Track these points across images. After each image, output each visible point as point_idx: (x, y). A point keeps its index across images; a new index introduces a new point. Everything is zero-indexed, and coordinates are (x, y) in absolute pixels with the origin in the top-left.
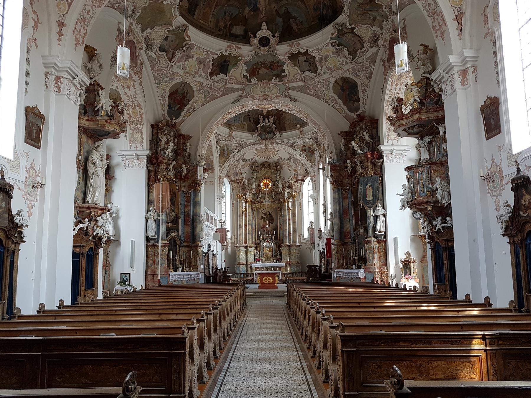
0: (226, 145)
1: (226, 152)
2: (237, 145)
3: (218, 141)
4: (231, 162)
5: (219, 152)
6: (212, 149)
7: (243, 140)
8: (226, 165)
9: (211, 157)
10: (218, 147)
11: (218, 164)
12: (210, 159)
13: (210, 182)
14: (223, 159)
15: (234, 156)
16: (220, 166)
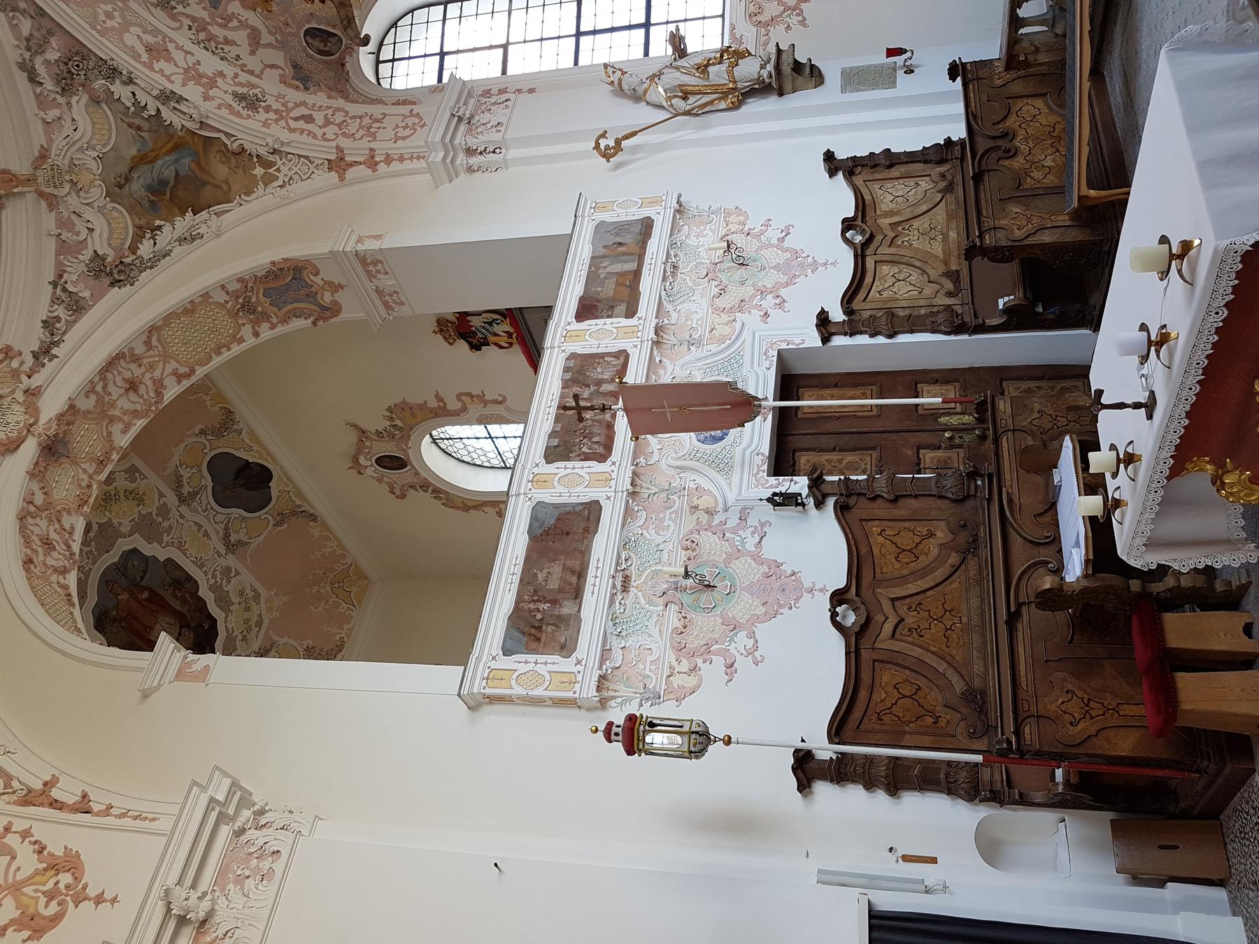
0: (117, 188)
1: (165, 167)
2: (80, 102)
3: (115, 272)
4: (209, 106)
5: (183, 223)
6: (168, 318)
7: (21, 77)
8: (252, 132)
9: (220, 297)
10: (145, 249)
11: (262, 199)
12: (235, 295)
13: (371, 276)
14: (220, 170)
15: (167, 97)
16: (268, 180)
